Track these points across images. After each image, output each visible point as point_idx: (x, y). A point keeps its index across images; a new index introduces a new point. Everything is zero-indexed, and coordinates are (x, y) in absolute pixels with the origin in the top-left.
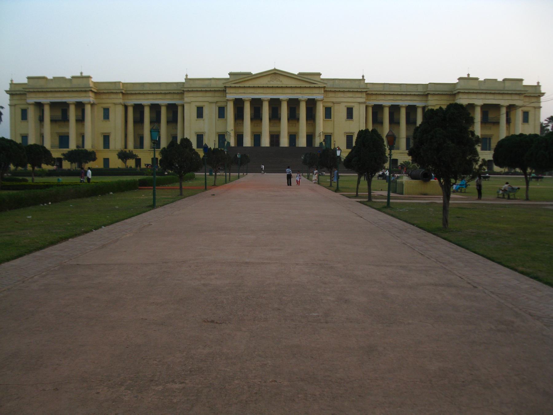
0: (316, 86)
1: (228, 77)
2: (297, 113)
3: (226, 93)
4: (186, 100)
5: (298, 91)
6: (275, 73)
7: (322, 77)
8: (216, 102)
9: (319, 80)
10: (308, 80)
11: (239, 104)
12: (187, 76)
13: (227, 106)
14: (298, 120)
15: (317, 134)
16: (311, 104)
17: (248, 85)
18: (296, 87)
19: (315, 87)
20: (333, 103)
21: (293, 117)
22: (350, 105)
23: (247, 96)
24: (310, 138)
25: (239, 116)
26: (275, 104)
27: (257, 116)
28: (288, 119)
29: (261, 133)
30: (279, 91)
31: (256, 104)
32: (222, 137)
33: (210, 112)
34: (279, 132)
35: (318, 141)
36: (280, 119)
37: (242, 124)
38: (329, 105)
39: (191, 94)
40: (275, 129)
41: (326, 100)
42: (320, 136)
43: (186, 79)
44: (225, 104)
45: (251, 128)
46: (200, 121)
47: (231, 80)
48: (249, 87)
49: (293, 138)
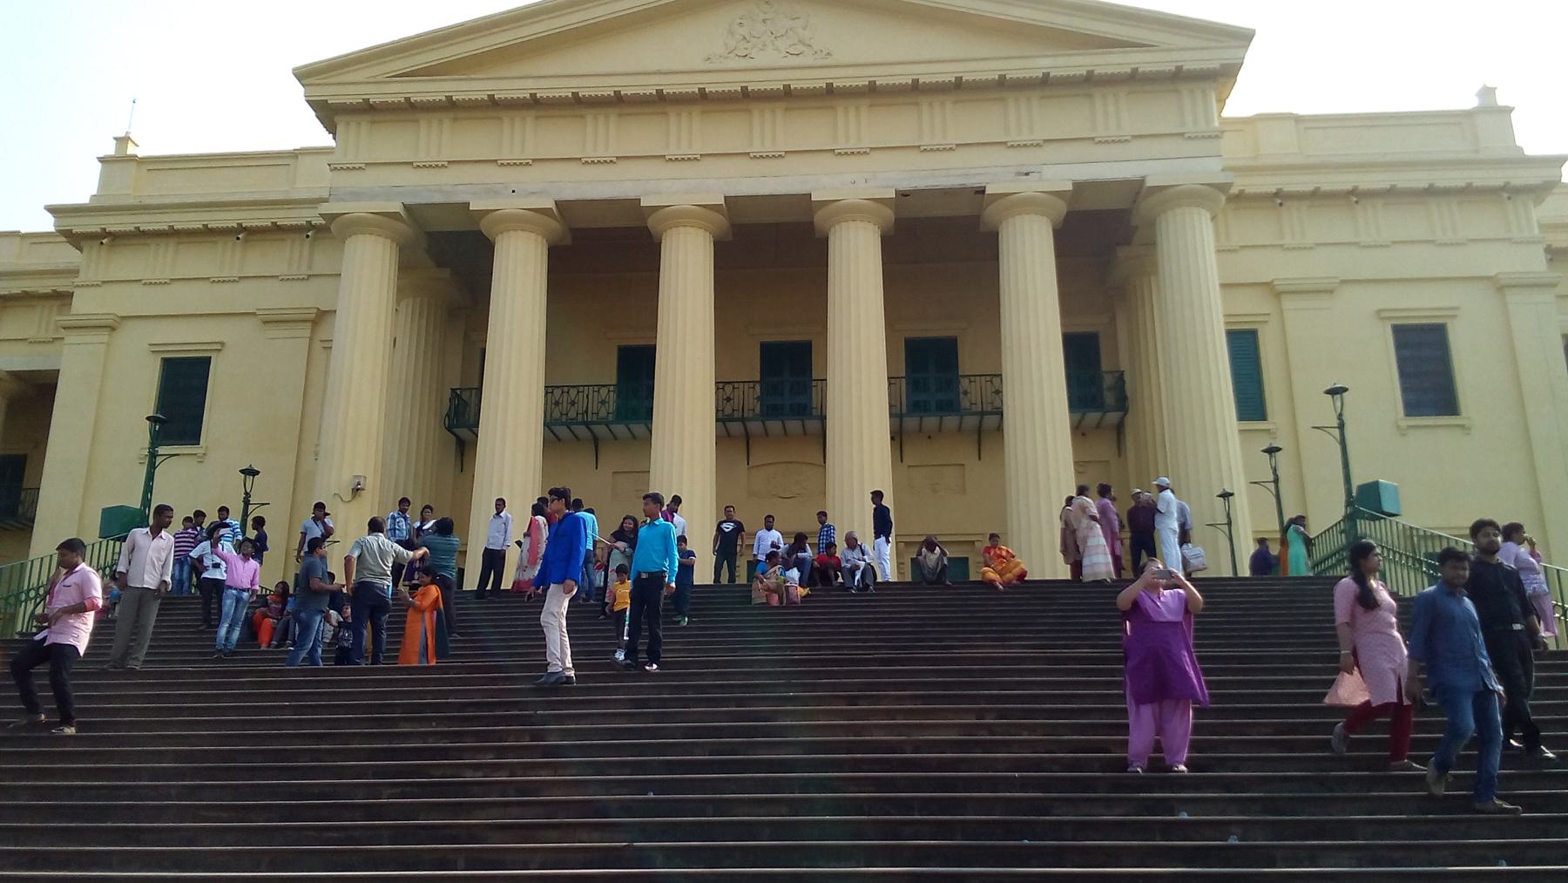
0: (1145, 62)
2: (969, 362)
4: (84, 304)
11: (447, 262)
12: (123, 141)
14: (987, 427)
18: (958, 88)
19: (1134, 80)
20: (1274, 291)
22: (1419, 305)
26: (771, 253)
28: (898, 437)
31: (604, 258)
39: (128, 264)
43: (118, 162)
48: (535, 105)
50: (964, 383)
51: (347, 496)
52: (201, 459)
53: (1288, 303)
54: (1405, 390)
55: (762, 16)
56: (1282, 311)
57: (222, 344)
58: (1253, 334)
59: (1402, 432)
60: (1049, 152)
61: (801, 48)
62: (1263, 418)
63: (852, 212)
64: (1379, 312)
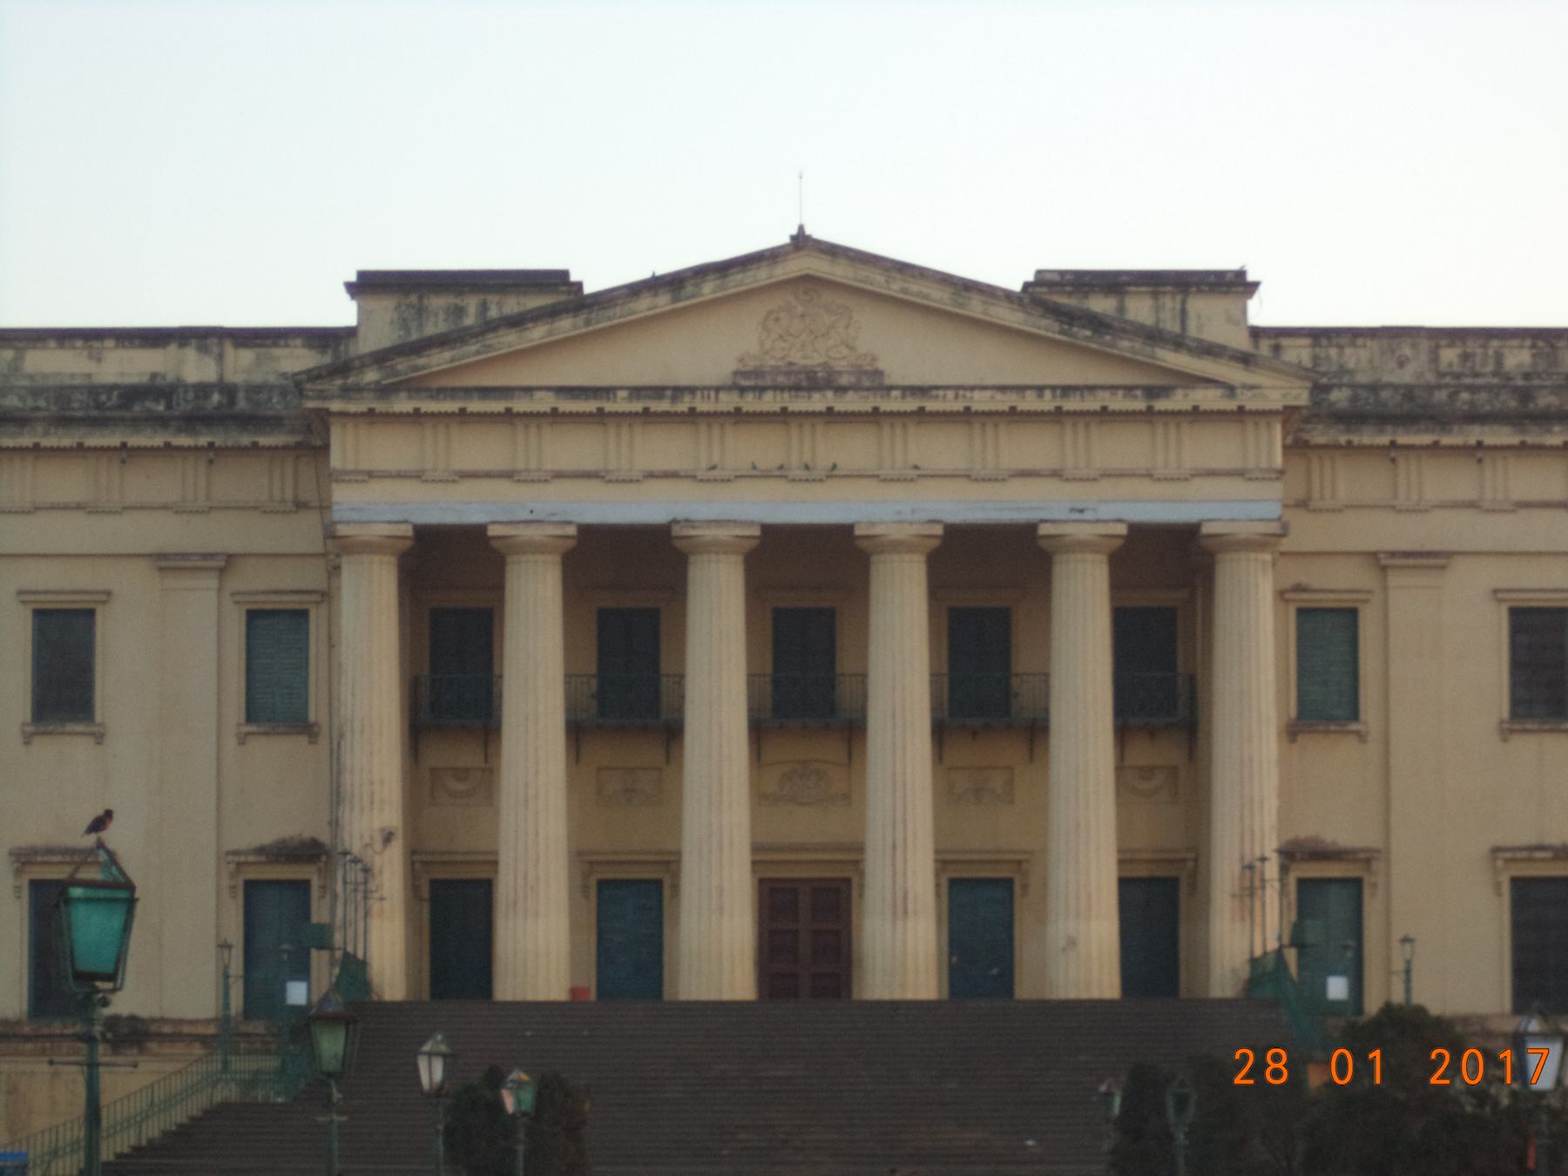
0: (1209, 399)
1: (344, 313)
2: (1023, 661)
3: (330, 477)
5: (1035, 448)
6: (808, 282)
7: (1263, 312)
8: (224, 564)
9: (1242, 343)
10: (1126, 334)
13: (327, 596)
14: (1036, 731)
15: (1224, 873)
16: (1165, 581)
17: (543, 403)
19: (1196, 415)
20: (1382, 562)
21: (986, 698)
23: (537, 493)
24: (1158, 907)
25: (453, 692)
27: (627, 699)
28: (940, 732)
29: (671, 863)
30: (854, 449)
32: (281, 898)
33: (168, 660)
34: (854, 854)
35: (1239, 935)
36: (853, 730)
37: (486, 779)
38: (1338, 581)
40: (806, 826)
41: (1308, 533)
42: (1250, 889)
44: (312, 577)
45: (578, 817)
46: (68, 752)
47: (367, 344)
49: (985, 909)
50: (1015, 682)
51: (378, 846)
52: (99, 738)
53: (1394, 579)
54: (1515, 684)
55: (800, 309)
56: (1385, 589)
57: (109, 593)
58: (1349, 617)
59: (1506, 732)
60: (1106, 485)
61: (845, 351)
62: (1355, 715)
63: (898, 547)
64: (1496, 591)
